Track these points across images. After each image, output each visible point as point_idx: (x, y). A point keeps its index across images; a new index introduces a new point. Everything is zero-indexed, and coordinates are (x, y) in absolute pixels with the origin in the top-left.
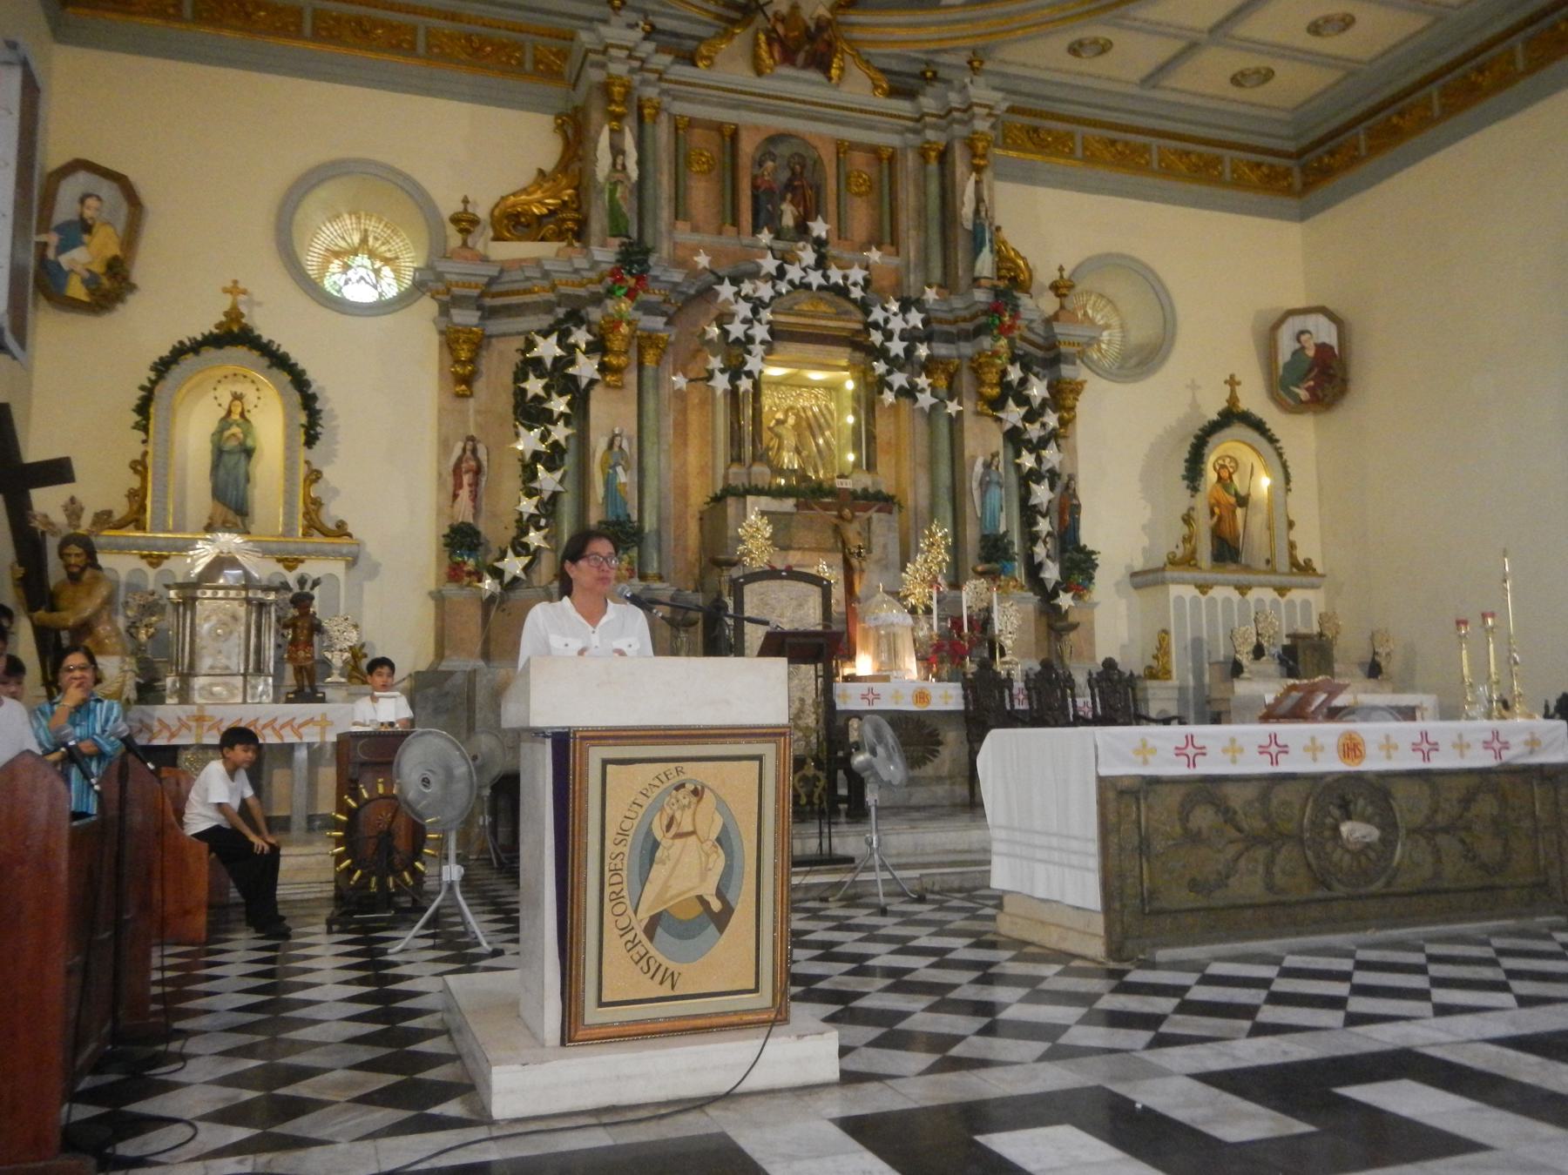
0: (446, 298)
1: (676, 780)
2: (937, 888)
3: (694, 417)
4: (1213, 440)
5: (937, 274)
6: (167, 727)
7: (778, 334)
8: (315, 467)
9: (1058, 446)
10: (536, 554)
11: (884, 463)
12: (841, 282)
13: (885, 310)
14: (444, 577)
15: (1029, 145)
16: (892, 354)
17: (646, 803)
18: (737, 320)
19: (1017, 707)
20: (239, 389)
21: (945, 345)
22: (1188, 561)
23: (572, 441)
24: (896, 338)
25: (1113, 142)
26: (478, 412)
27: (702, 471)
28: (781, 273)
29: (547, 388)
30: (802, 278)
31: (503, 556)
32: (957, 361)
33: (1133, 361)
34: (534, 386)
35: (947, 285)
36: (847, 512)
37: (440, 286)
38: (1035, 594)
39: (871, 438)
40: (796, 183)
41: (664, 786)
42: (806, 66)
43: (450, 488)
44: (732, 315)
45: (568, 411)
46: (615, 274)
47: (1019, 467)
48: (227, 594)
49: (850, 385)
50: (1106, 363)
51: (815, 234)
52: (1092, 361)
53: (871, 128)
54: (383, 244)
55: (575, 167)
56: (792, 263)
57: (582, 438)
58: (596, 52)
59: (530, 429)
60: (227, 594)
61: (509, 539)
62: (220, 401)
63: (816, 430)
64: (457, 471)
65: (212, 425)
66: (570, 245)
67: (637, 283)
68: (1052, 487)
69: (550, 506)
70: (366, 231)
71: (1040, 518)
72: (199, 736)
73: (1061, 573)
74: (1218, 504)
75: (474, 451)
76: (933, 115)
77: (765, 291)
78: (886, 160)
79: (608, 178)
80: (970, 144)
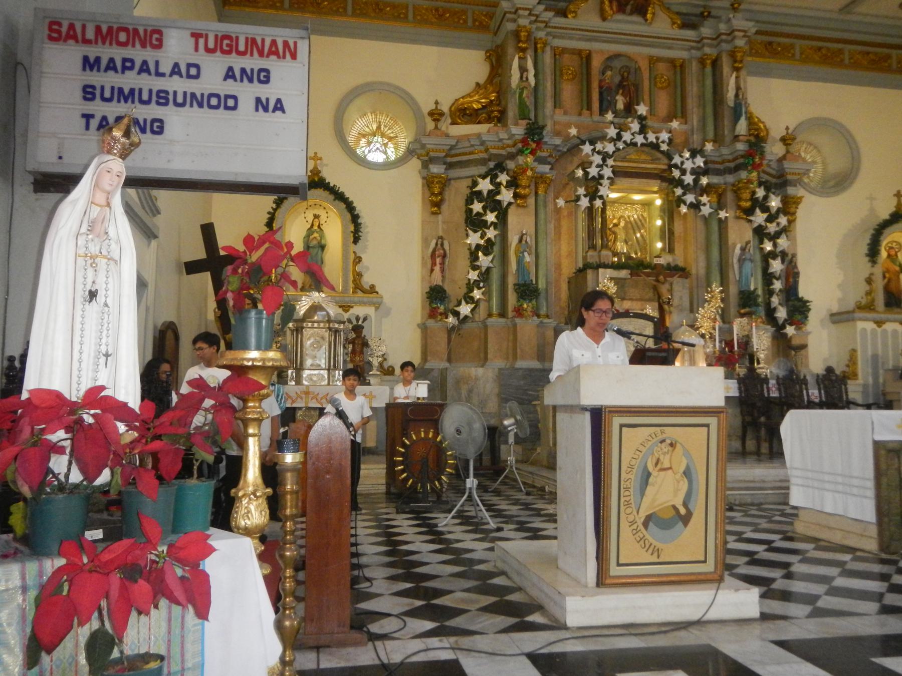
0: (426, 158)
1: (660, 437)
2: (737, 502)
3: (565, 224)
4: (887, 231)
5: (711, 134)
6: (289, 397)
7: (618, 173)
8: (358, 255)
9: (787, 236)
10: (477, 303)
11: (679, 248)
12: (655, 141)
13: (681, 156)
14: (427, 316)
15: (767, 54)
16: (686, 183)
17: (644, 450)
18: (594, 165)
19: (772, 395)
20: (317, 212)
21: (717, 177)
22: (867, 307)
23: (498, 238)
24: (688, 173)
25: (820, 49)
26: (444, 222)
27: (569, 254)
28: (619, 137)
29: (484, 208)
30: (632, 139)
31: (459, 304)
32: (724, 187)
33: (832, 183)
35: (717, 140)
36: (661, 278)
37: (423, 152)
38: (772, 327)
39: (671, 233)
40: (625, 83)
41: (654, 441)
42: (631, 14)
43: (429, 266)
44: (591, 163)
45: (495, 221)
46: (524, 141)
47: (762, 249)
48: (319, 325)
49: (659, 202)
50: (812, 184)
51: (639, 113)
52: (805, 183)
53: (670, 48)
54: (389, 129)
55: (497, 80)
56: (626, 131)
57: (504, 237)
58: (510, 13)
59: (475, 231)
60: (319, 325)
61: (463, 294)
62: (307, 219)
63: (636, 228)
64: (433, 255)
65: (304, 233)
66: (496, 125)
67: (537, 146)
68: (783, 262)
69: (486, 275)
70: (380, 122)
71: (775, 281)
72: (307, 403)
73: (788, 314)
74: (888, 271)
75: (442, 245)
76: (708, 38)
77: (610, 148)
78: (678, 67)
79: (518, 86)
80: (732, 54)
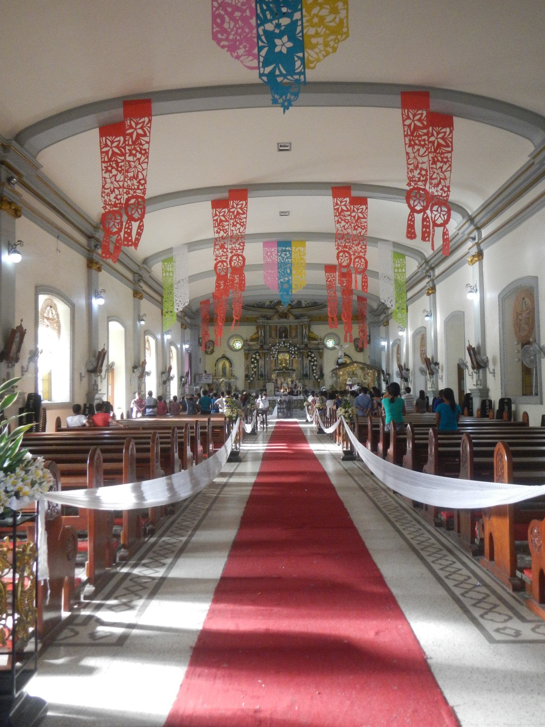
7: (279, 352)
10: (254, 378)
34: (253, 360)
69: (255, 372)
77: (277, 348)
78: (297, 326)
